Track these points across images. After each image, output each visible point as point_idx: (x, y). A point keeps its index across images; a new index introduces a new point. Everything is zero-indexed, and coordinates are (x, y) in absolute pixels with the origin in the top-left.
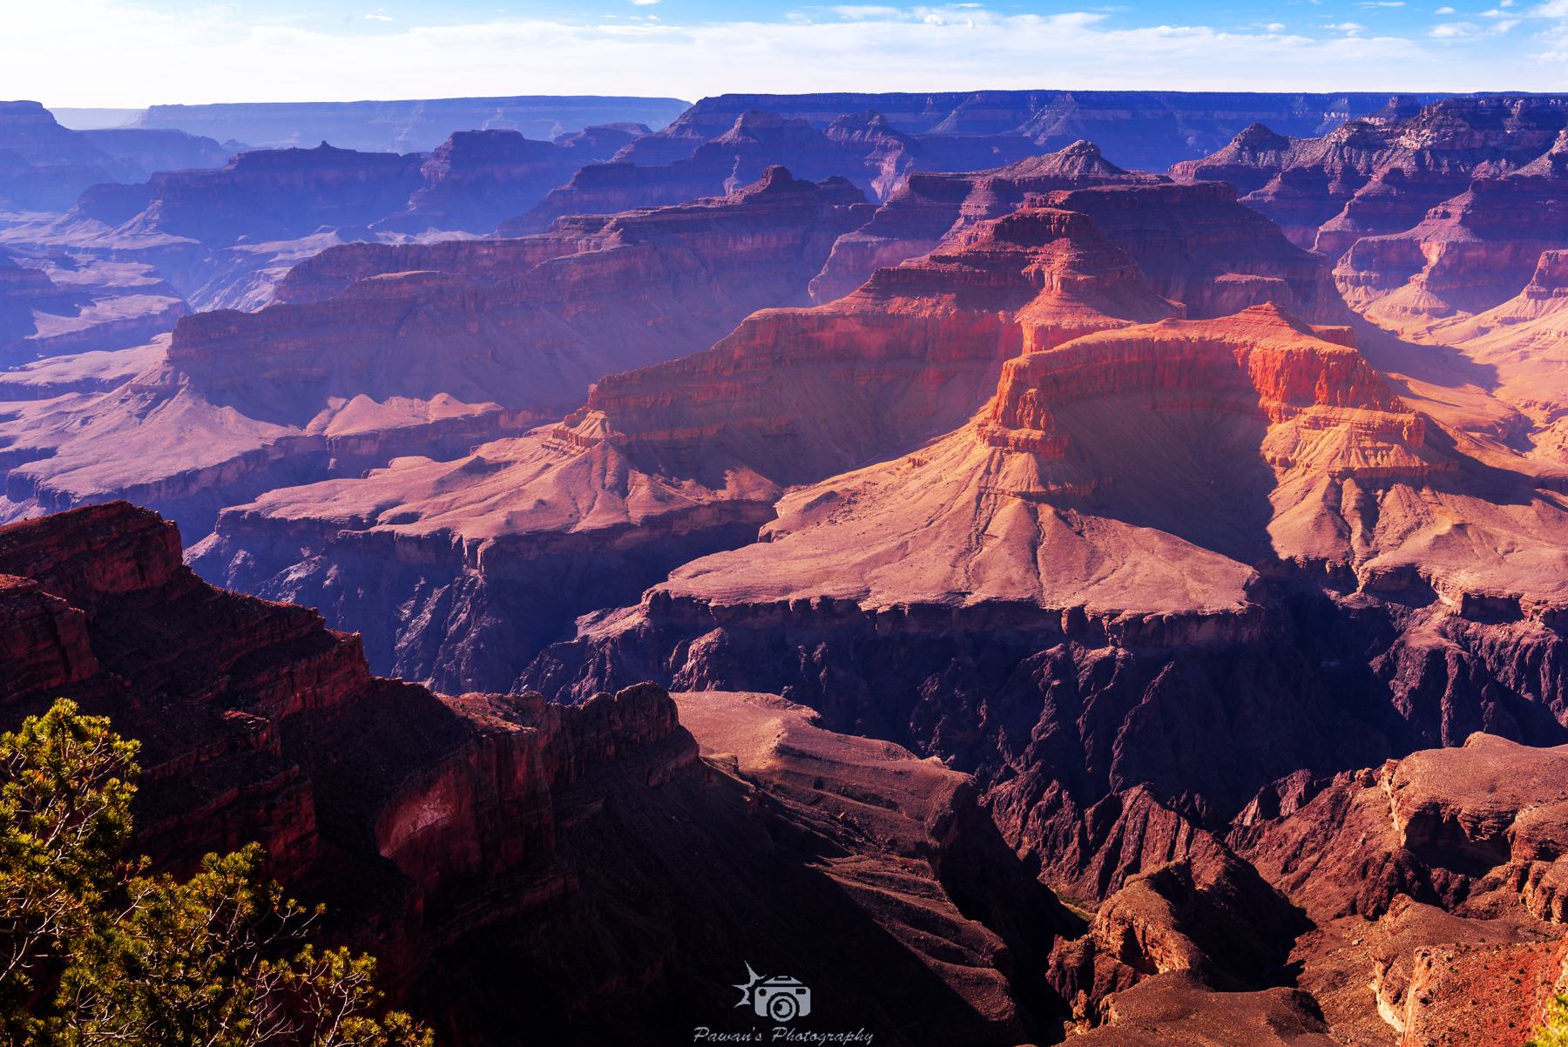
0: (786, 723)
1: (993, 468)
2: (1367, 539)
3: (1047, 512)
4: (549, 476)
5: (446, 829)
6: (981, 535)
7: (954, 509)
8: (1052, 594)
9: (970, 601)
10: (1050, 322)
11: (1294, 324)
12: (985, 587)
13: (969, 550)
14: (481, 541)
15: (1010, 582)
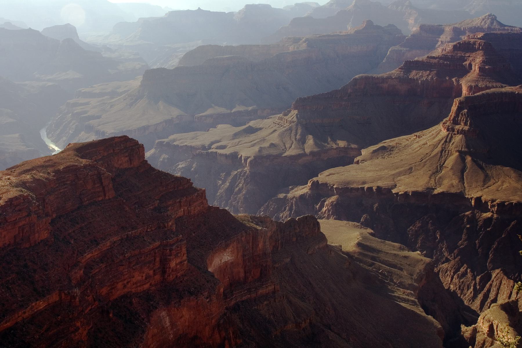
0: (361, 234)
1: (448, 140)
3: (469, 159)
4: (276, 134)
5: (232, 263)
6: (441, 167)
7: (432, 155)
8: (469, 191)
9: (436, 192)
12: (442, 187)
13: (437, 172)
15: (452, 186)
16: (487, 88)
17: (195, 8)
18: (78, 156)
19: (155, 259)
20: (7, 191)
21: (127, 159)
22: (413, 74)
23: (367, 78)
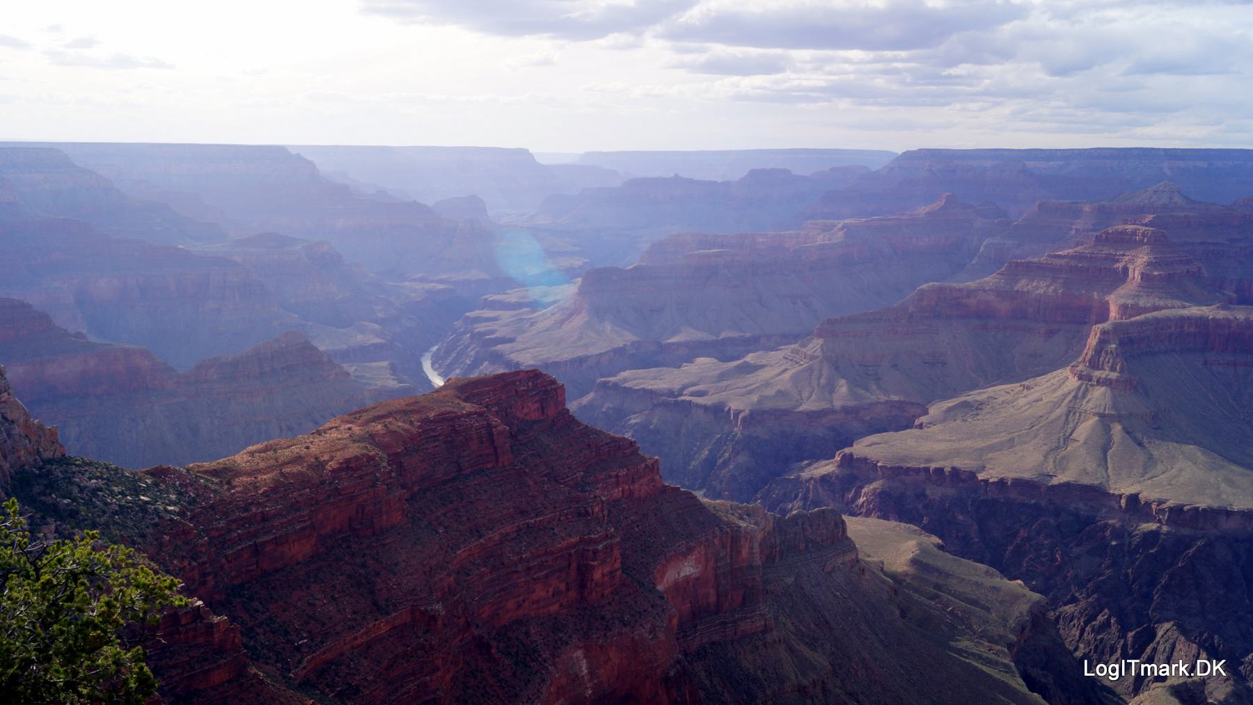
0: (919, 544)
1: (1080, 394)
3: (1117, 429)
4: (787, 376)
5: (698, 579)
6: (1067, 439)
8: (1116, 483)
9: (1055, 481)
10: (1130, 302)
13: (1058, 448)
15: (1085, 472)
18: (459, 398)
19: (569, 565)
20: (345, 447)
21: (536, 406)
22: (1022, 285)
23: (940, 289)
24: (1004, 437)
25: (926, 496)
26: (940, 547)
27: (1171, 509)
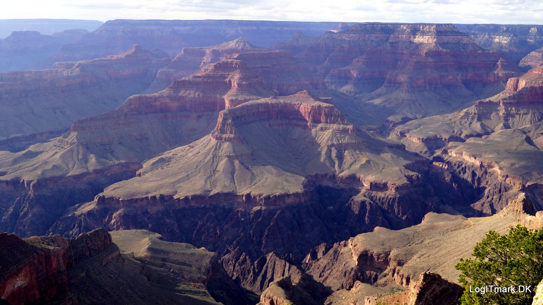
0: (150, 239)
1: (218, 147)
2: (340, 166)
3: (237, 162)
4: (57, 156)
5: (26, 287)
6: (215, 171)
7: (206, 161)
8: (239, 189)
9: (212, 193)
10: (234, 98)
11: (313, 97)
12: (217, 188)
13: (211, 176)
14: (31, 181)
15: (225, 186)
16: (246, 100)
17: (19, 31)
23: (140, 98)
24: (184, 174)
25: (148, 213)
26: (161, 239)
27: (265, 198)
